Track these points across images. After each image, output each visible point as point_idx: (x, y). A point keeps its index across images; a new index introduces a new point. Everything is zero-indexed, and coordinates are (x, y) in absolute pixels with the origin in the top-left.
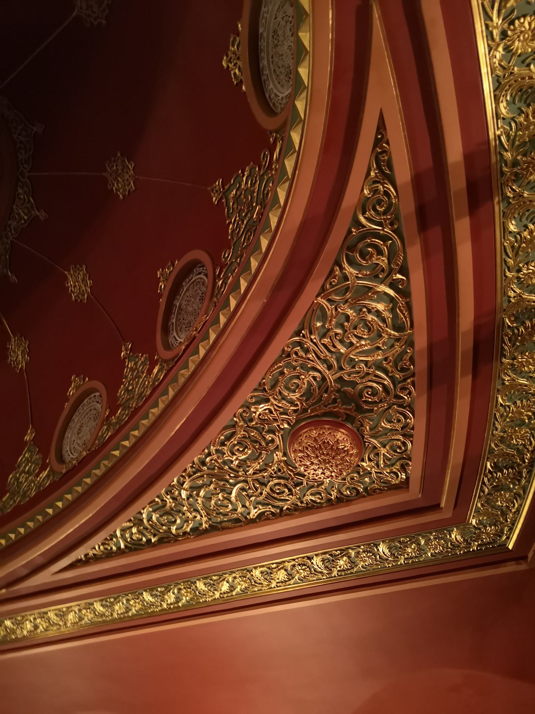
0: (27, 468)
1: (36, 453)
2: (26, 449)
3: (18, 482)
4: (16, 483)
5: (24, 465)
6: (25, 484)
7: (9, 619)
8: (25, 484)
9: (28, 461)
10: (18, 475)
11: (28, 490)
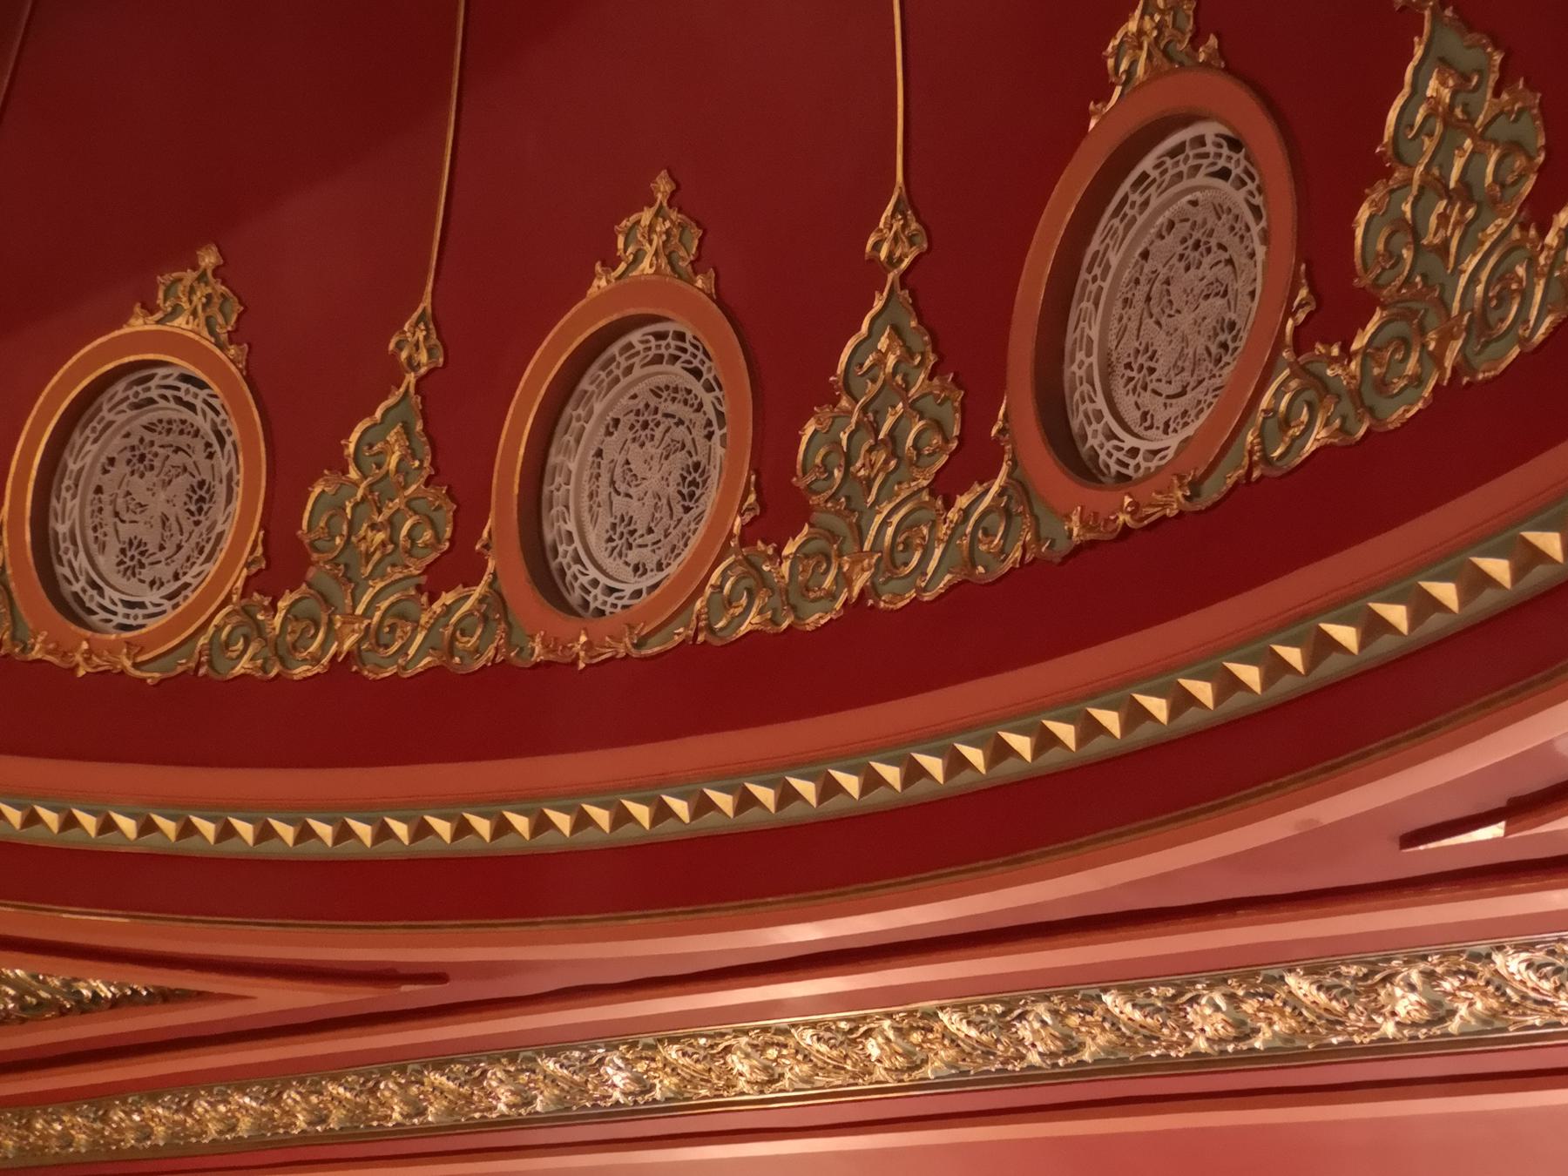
0: (1458, 165)
1: (1493, 78)
2: (1419, 52)
3: (1418, 249)
4: (1407, 254)
5: (1429, 145)
6: (1471, 264)
7: (1519, 948)
8: (1471, 264)
9: (1453, 123)
10: (1407, 208)
11: (1503, 300)
